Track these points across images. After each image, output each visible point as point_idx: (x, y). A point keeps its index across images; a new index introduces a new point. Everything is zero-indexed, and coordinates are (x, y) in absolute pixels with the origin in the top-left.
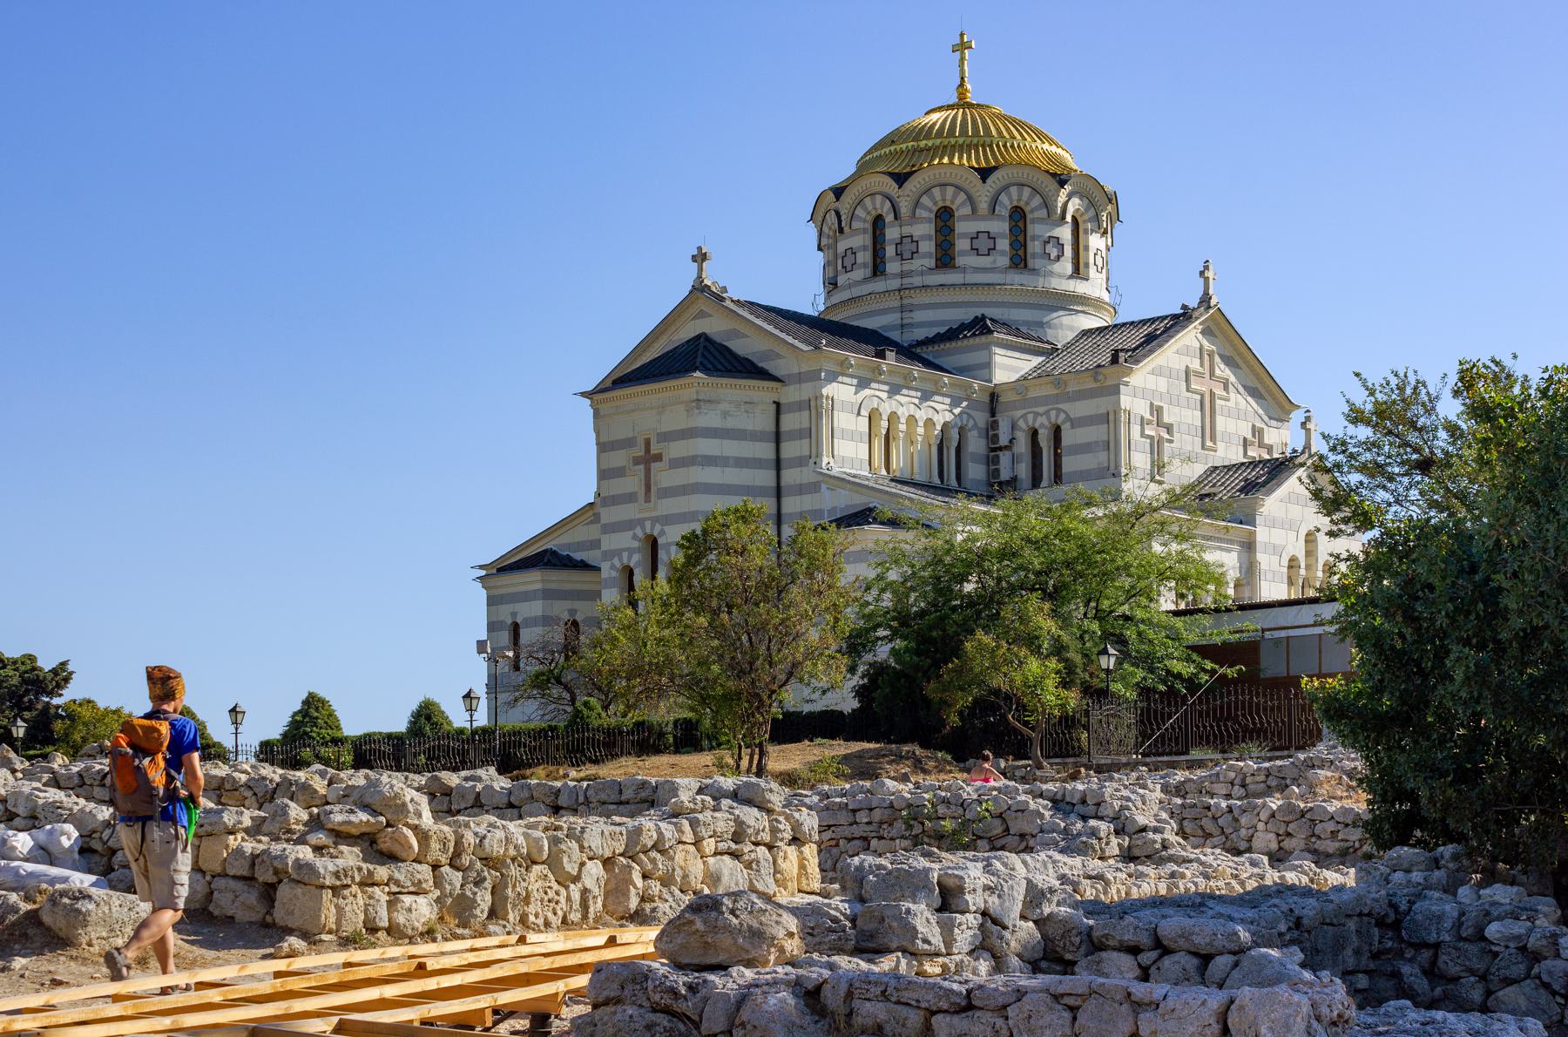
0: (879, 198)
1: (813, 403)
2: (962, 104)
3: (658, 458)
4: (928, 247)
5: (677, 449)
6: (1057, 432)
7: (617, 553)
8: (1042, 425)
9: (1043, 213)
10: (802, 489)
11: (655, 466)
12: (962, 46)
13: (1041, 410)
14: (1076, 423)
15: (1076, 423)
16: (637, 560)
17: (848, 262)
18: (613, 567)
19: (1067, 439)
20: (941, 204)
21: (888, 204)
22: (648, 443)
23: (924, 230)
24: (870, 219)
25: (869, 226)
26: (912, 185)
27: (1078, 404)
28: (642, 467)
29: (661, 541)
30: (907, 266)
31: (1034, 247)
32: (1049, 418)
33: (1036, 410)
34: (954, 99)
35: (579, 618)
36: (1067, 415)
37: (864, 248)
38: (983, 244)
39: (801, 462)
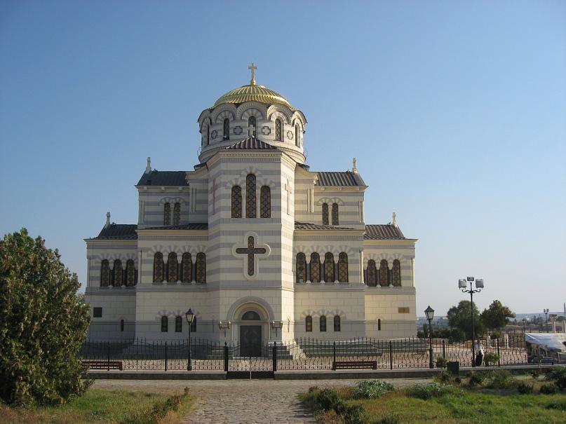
0: (255, 111)
2: (252, 85)
4: (274, 131)
6: (335, 206)
9: (301, 129)
12: (252, 68)
14: (344, 204)
17: (238, 131)
19: (340, 209)
21: (259, 114)
23: (273, 125)
30: (266, 137)
31: (301, 141)
34: (249, 84)
37: (245, 127)
38: (291, 136)
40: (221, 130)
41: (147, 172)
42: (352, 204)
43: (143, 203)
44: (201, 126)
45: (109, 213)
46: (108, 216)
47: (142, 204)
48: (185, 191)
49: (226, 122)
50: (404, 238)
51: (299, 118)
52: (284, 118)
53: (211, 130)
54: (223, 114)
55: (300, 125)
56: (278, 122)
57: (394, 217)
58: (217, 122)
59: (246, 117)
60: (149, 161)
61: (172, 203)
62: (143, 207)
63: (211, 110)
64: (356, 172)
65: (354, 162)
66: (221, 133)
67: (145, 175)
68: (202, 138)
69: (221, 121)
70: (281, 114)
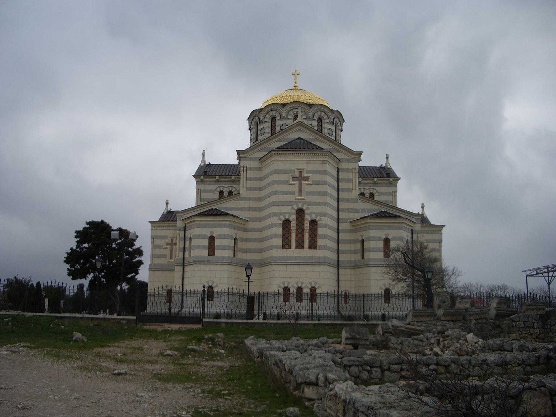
1: (354, 170)
3: (307, 179)
5: (314, 177)
7: (284, 214)
8: (367, 193)
9: (340, 128)
10: (348, 201)
11: (304, 182)
13: (367, 188)
15: (380, 194)
16: (293, 218)
18: (280, 219)
20: (319, 117)
22: (300, 172)
24: (294, 116)
25: (293, 118)
26: (313, 109)
27: (381, 188)
28: (297, 182)
29: (306, 212)
32: (370, 191)
33: (364, 187)
35: (238, 237)
36: (377, 191)
38: (331, 133)
39: (349, 190)
40: (268, 127)
41: (202, 164)
42: (386, 194)
43: (199, 191)
44: (250, 125)
45: (167, 201)
46: (167, 204)
47: (199, 191)
48: (237, 180)
49: (273, 119)
50: (431, 225)
51: (338, 118)
52: (326, 117)
53: (260, 127)
54: (271, 113)
55: (339, 124)
56: (319, 121)
57: (423, 207)
58: (266, 120)
59: (291, 115)
60: (204, 155)
61: (226, 191)
62: (199, 194)
63: (261, 110)
64: (389, 167)
65: (387, 158)
66: (269, 130)
67: (200, 167)
68: (251, 135)
69: (268, 119)
70: (323, 114)
